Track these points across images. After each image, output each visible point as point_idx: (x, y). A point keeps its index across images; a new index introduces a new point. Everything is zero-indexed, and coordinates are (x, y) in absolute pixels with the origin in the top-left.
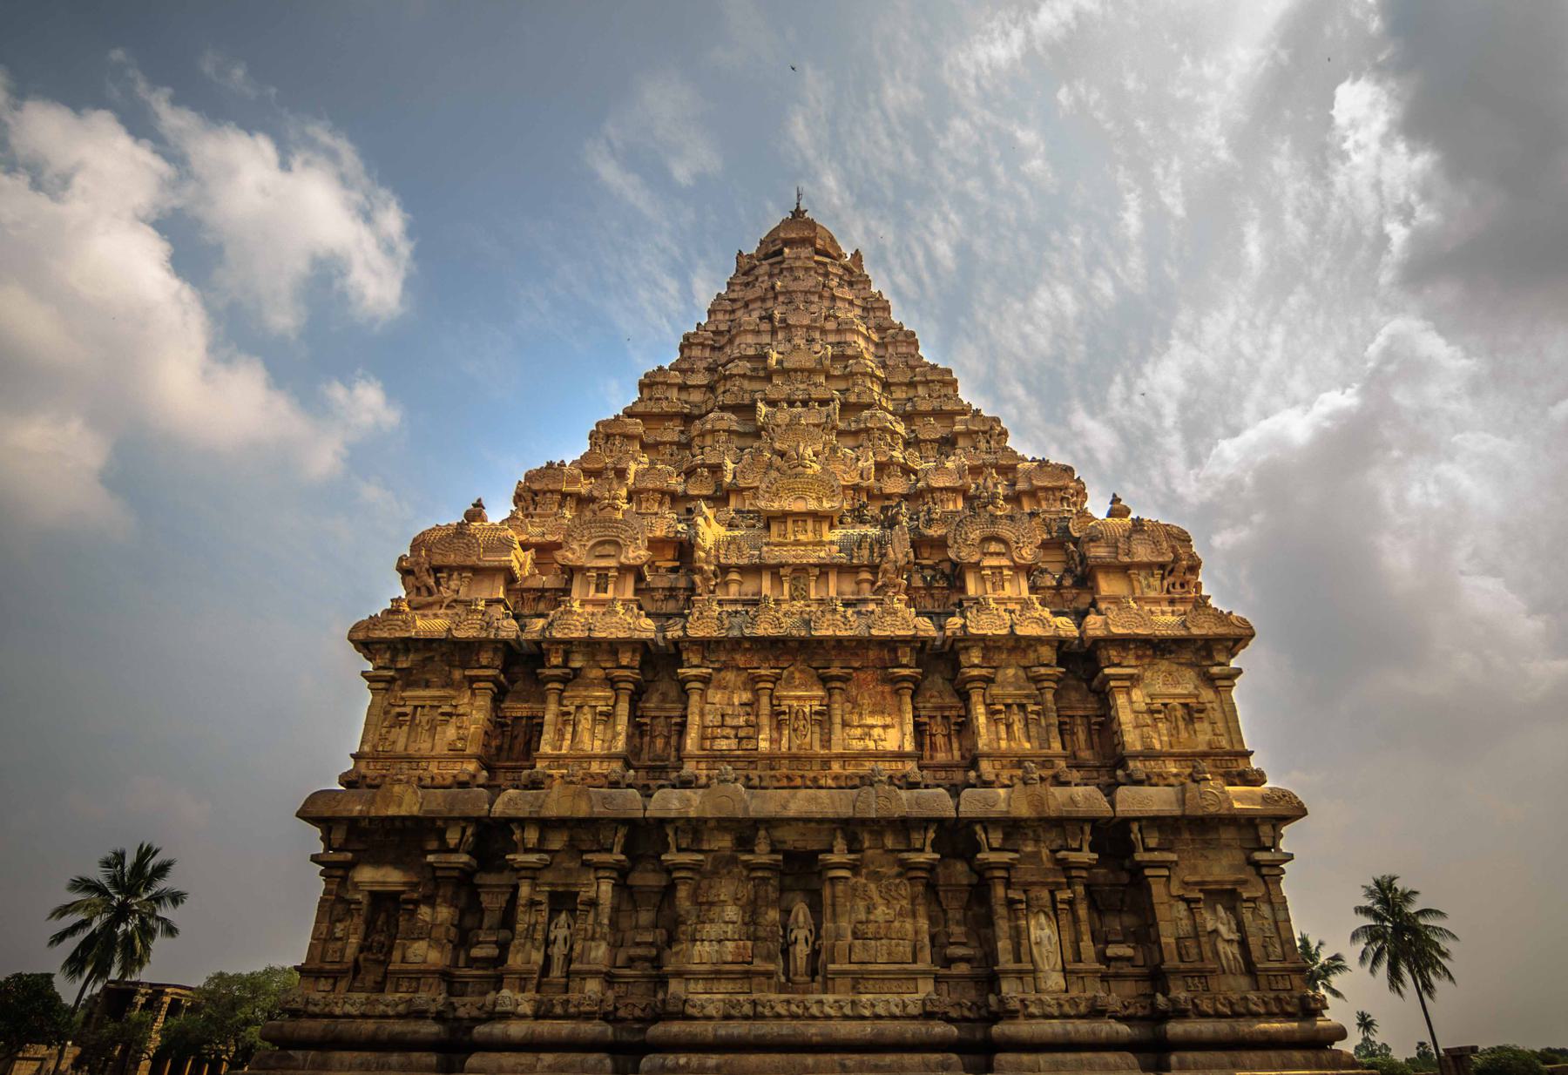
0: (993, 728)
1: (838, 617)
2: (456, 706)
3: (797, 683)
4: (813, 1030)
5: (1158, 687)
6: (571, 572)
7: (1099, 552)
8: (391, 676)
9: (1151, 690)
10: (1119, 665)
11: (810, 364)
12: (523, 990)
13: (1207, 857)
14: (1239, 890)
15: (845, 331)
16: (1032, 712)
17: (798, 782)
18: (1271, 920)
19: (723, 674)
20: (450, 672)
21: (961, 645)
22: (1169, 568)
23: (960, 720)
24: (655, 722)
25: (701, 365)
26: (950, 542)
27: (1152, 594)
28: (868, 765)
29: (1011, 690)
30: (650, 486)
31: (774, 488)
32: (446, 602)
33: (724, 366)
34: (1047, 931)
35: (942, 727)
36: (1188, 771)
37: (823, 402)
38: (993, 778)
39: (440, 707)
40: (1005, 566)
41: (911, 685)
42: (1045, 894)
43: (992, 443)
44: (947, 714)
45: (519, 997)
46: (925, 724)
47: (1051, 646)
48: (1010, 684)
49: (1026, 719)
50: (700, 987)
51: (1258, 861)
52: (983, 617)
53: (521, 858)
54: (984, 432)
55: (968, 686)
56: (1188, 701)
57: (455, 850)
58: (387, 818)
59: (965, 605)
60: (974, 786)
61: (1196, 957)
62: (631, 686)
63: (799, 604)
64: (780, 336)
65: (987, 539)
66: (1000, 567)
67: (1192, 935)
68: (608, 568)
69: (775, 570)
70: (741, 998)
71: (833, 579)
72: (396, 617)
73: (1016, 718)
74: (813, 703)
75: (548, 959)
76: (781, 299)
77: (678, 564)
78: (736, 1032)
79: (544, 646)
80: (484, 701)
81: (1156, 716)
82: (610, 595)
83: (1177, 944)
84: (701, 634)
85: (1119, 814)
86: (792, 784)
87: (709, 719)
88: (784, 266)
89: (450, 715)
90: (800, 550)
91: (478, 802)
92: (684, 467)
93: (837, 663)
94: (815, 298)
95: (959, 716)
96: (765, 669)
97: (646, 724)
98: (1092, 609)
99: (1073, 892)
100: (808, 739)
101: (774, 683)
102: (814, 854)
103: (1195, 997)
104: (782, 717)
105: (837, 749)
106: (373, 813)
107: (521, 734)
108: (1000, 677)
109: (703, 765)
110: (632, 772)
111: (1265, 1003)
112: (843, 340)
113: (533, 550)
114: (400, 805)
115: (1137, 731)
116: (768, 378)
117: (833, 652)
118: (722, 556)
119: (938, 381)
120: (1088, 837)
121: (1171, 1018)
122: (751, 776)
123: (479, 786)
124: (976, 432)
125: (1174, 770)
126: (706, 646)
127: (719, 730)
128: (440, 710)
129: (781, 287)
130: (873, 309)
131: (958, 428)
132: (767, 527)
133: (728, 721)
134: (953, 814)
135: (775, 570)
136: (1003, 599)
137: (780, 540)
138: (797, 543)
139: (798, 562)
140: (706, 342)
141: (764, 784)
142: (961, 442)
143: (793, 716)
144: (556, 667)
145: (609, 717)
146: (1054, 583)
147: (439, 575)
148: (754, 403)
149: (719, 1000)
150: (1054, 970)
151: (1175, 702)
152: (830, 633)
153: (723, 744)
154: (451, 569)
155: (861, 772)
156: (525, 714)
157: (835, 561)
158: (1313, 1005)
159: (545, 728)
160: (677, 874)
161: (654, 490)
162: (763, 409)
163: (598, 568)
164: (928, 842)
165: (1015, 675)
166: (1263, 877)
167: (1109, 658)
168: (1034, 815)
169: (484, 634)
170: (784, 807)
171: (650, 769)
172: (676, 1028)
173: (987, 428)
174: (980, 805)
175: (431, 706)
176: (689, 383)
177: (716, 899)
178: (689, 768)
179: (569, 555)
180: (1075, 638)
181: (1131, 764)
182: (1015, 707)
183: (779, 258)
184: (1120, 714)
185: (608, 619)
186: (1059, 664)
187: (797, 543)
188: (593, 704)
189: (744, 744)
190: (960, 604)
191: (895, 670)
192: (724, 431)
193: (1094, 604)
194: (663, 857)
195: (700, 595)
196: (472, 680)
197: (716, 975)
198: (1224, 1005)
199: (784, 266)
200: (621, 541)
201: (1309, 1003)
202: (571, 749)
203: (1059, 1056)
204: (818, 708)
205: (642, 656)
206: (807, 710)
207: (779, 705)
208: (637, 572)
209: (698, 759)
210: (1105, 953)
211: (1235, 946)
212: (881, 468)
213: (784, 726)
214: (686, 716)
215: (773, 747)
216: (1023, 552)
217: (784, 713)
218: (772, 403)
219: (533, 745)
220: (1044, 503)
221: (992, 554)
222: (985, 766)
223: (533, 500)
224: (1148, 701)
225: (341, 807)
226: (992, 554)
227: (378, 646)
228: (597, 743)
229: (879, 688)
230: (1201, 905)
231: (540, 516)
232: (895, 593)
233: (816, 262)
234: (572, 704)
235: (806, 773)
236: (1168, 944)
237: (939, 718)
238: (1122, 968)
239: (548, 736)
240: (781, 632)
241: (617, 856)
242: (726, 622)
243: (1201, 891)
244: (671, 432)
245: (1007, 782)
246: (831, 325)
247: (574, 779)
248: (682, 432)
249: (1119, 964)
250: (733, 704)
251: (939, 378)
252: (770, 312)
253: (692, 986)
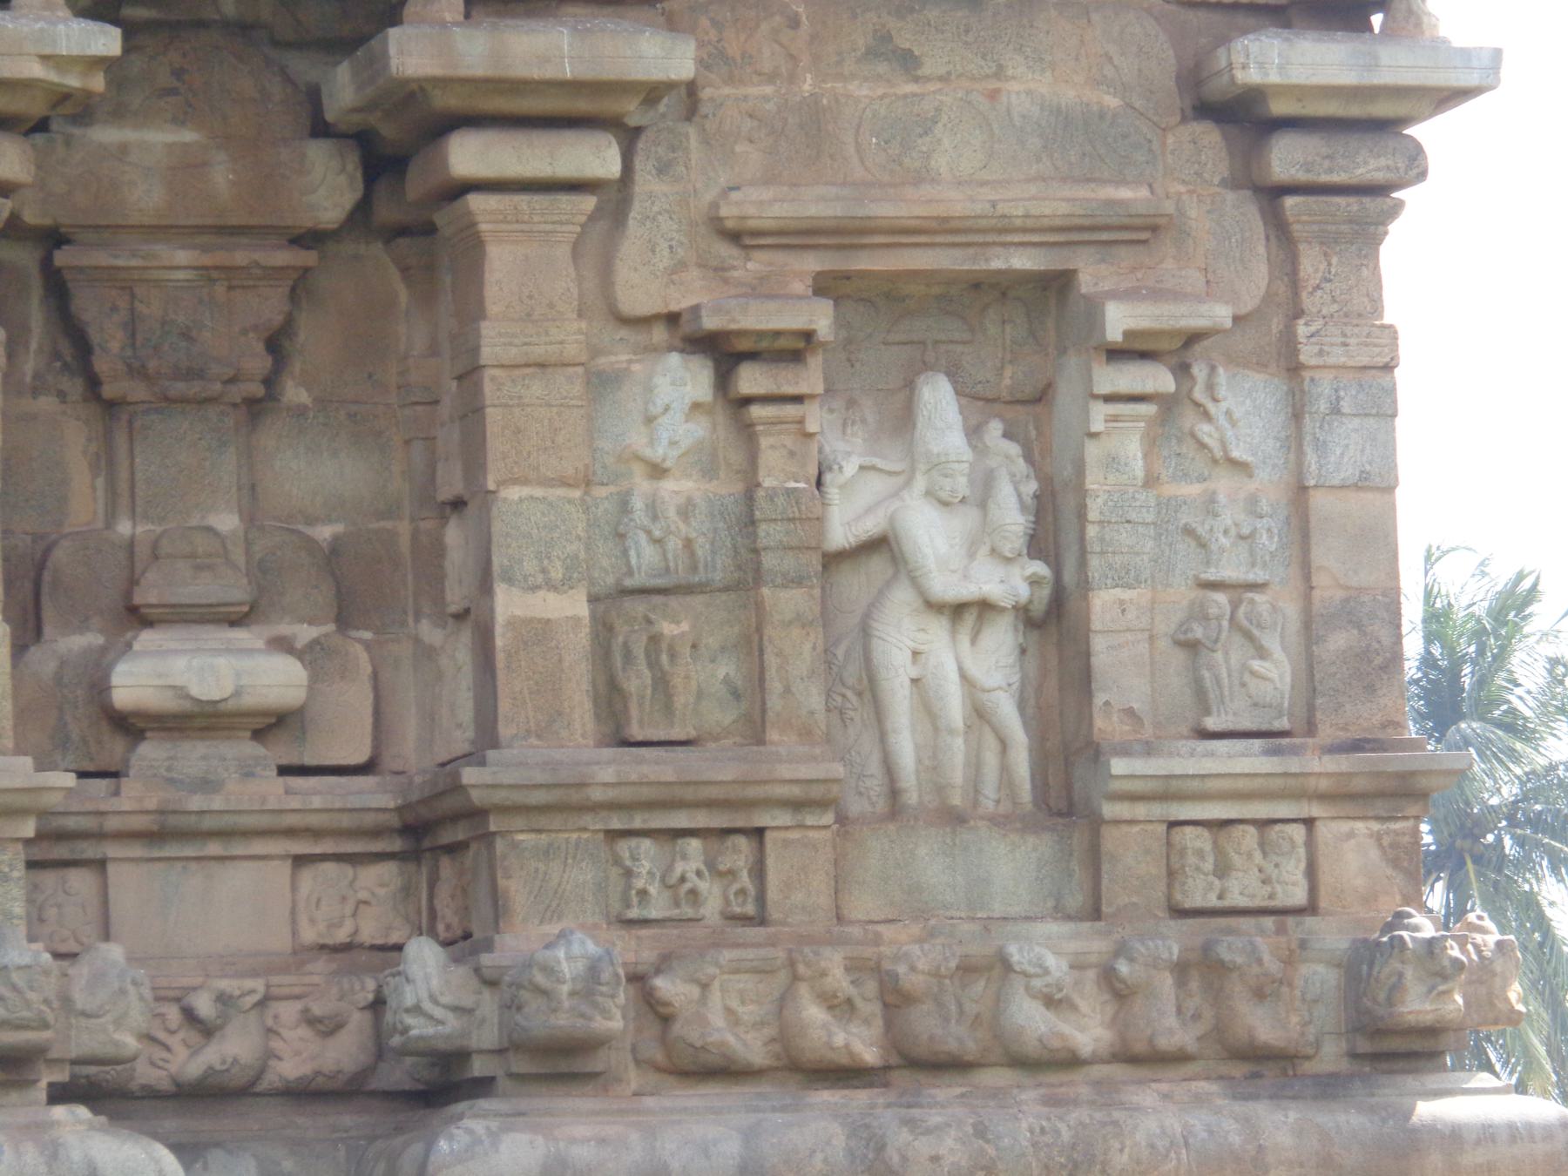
13: (908, 62)
14: (1091, 275)
18: (1269, 481)
51: (1256, 95)
61: (720, 715)
67: (720, 569)
83: (603, 629)
103: (664, 964)
111: (1118, 992)
121: (483, 1087)
158: (1416, 1006)
198: (842, 1007)
201: (1397, 987)
210: (100, 688)
211: (1001, 639)
230: (809, 378)
236: (539, 632)
238: (207, 785)
243: (824, 286)
249: (194, 756)
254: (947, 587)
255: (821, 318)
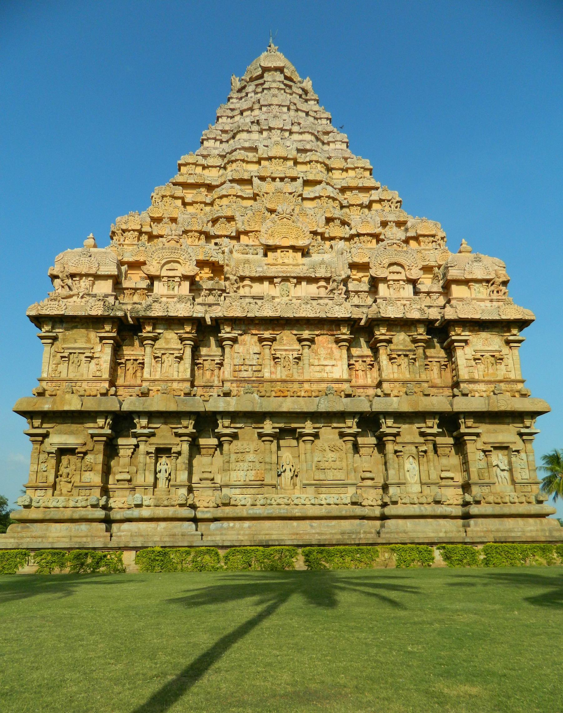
0: (391, 367)
1: (309, 306)
2: (93, 353)
3: (285, 342)
4: (297, 512)
5: (479, 347)
6: (152, 278)
7: (453, 273)
8: (54, 336)
9: (476, 348)
10: (459, 335)
11: (284, 154)
12: (145, 494)
15: (304, 133)
16: (412, 359)
17: (286, 393)
19: (243, 337)
20: (88, 334)
21: (375, 323)
22: (491, 282)
23: (372, 363)
24: (205, 362)
25: (216, 152)
26: (371, 265)
27: (480, 296)
28: (323, 386)
29: (401, 347)
30: (194, 229)
31: (270, 232)
32: (81, 294)
33: (230, 153)
34: (414, 465)
35: (362, 366)
36: (491, 389)
37: (294, 179)
38: (389, 392)
39: (84, 353)
40: (401, 280)
41: (347, 344)
42: (414, 448)
43: (392, 207)
44: (365, 359)
45: (145, 497)
46: (353, 365)
47: (425, 325)
48: (401, 344)
49: (409, 362)
50: (238, 491)
52: (389, 307)
53: (138, 430)
54: (389, 201)
55: (378, 345)
56: (494, 354)
57: (102, 428)
58: (64, 411)
59: (378, 301)
60: (379, 396)
62: (192, 343)
63: (285, 299)
64: (265, 134)
65: (391, 265)
66: (398, 280)
68: (174, 277)
69: (271, 279)
70: (259, 496)
71: (304, 284)
72: (54, 303)
73: (403, 362)
74: (294, 353)
75: (156, 479)
76: (264, 109)
77: (212, 275)
78: (258, 512)
79: (141, 321)
80: (108, 350)
81: (477, 361)
82: (176, 292)
84: (231, 315)
85: (455, 410)
86: (282, 395)
87: (237, 361)
88: (265, 86)
89: (92, 358)
90: (285, 268)
91: (111, 405)
92: (211, 218)
93: (307, 332)
94: (285, 109)
95: (371, 361)
96: (267, 334)
97: (200, 364)
98: (447, 305)
99: (428, 447)
100: (291, 372)
101: (272, 342)
102: (296, 429)
104: (276, 360)
105: (307, 377)
106: (55, 409)
107: (131, 369)
108: (395, 340)
109: (234, 385)
110: (195, 388)
111: (518, 498)
112: (304, 139)
113: (126, 266)
114: (70, 404)
115: (467, 369)
116: (259, 162)
117: (305, 326)
118: (241, 271)
119: (362, 168)
120: (437, 421)
122: (261, 391)
123: (111, 395)
124: (384, 200)
125: (484, 389)
126: (234, 322)
127: (242, 367)
128: (85, 355)
129: (264, 101)
130: (321, 118)
131: (373, 198)
132: (266, 255)
133: (247, 362)
134: (369, 410)
135: (271, 280)
136: (399, 298)
137: (274, 262)
138: (283, 264)
139: (284, 275)
140: (218, 138)
141: (267, 395)
142: (375, 206)
143: (282, 360)
144: (149, 332)
145: (181, 358)
146: (427, 290)
147: (74, 279)
148: (252, 177)
149: (249, 498)
150: (416, 483)
151: (487, 355)
152: (303, 314)
153: (245, 374)
154: (81, 276)
155: (320, 389)
156: (132, 358)
157: (305, 275)
159: (145, 365)
160: (222, 439)
161: (196, 231)
162: (256, 181)
163: (169, 277)
164: (355, 424)
165: (404, 339)
166: (523, 440)
167: (455, 331)
168: (411, 410)
169: (106, 314)
170: (280, 406)
171: (204, 386)
172: (227, 509)
173: (390, 198)
174: (383, 405)
175: (79, 353)
176: (209, 164)
177: (244, 451)
178: (227, 386)
179: (151, 268)
180: (437, 320)
181: (462, 385)
182: (402, 356)
183: (261, 81)
184: (458, 360)
185: (178, 305)
186: (427, 334)
187: (283, 264)
188: (172, 352)
189: (256, 374)
190: (375, 301)
191: (339, 336)
192: (234, 195)
193: (449, 302)
194: (216, 431)
195: (228, 293)
196: (102, 339)
197: (246, 486)
199: (265, 86)
200: (181, 261)
202: (161, 376)
203: (417, 520)
204: (297, 356)
205: (197, 327)
206: (291, 357)
207: (275, 354)
208: (192, 280)
209: (232, 381)
212: (329, 220)
213: (278, 365)
214: (224, 360)
215: (272, 376)
216: (412, 271)
217: (278, 358)
218: (262, 179)
219: (139, 374)
220: (422, 244)
221: (394, 273)
222: (385, 385)
223: (122, 235)
224: (474, 353)
225: (37, 406)
226: (394, 273)
227: (43, 319)
228: (176, 374)
229: (330, 346)
231: (128, 245)
232: (340, 294)
233: (286, 85)
234: (160, 353)
235: (291, 389)
237: (360, 362)
239: (146, 370)
240: (277, 314)
241: (191, 429)
242: (246, 308)
243: (492, 447)
244: (202, 195)
245: (397, 394)
246: (296, 128)
247: (165, 392)
248: (206, 195)
250: (250, 353)
251: (363, 165)
252: (257, 118)
253: (233, 491)
254: (502, 468)
255: (492, 449)
